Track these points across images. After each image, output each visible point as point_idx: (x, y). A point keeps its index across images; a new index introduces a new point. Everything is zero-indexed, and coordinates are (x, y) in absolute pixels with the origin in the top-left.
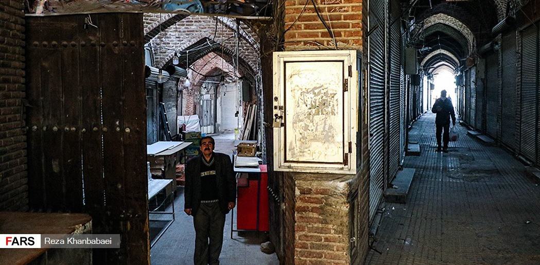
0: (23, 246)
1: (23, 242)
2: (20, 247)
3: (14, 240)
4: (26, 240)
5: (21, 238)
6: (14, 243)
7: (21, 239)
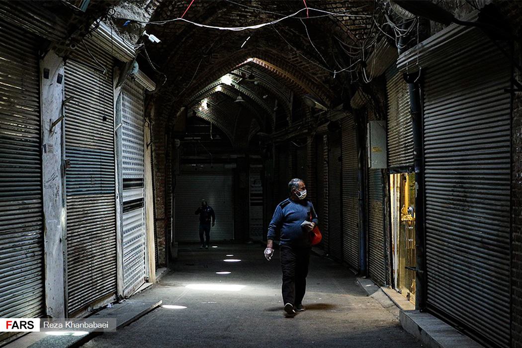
0: (23, 330)
1: (22, 326)
2: (19, 330)
3: (14, 324)
4: (26, 324)
5: (21, 322)
6: (14, 326)
7: (21, 323)
